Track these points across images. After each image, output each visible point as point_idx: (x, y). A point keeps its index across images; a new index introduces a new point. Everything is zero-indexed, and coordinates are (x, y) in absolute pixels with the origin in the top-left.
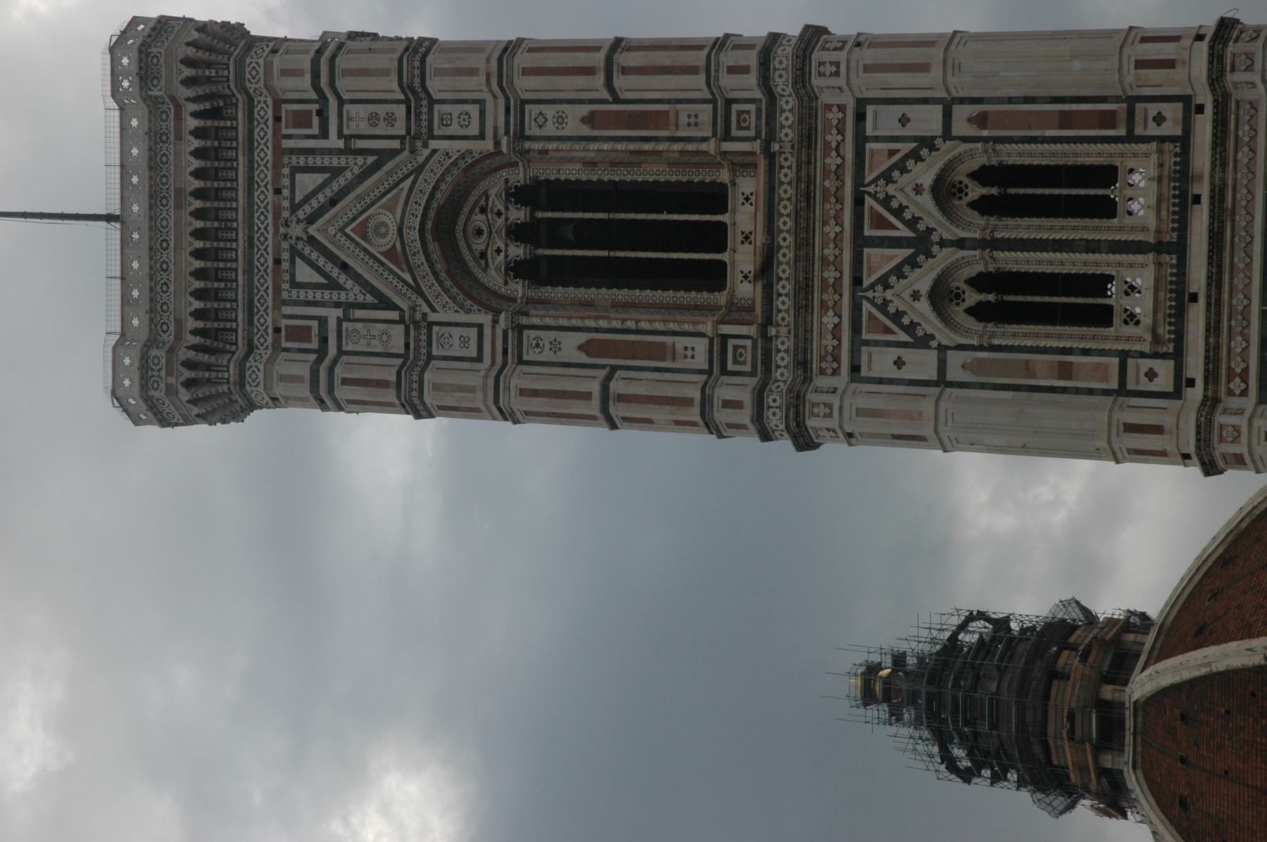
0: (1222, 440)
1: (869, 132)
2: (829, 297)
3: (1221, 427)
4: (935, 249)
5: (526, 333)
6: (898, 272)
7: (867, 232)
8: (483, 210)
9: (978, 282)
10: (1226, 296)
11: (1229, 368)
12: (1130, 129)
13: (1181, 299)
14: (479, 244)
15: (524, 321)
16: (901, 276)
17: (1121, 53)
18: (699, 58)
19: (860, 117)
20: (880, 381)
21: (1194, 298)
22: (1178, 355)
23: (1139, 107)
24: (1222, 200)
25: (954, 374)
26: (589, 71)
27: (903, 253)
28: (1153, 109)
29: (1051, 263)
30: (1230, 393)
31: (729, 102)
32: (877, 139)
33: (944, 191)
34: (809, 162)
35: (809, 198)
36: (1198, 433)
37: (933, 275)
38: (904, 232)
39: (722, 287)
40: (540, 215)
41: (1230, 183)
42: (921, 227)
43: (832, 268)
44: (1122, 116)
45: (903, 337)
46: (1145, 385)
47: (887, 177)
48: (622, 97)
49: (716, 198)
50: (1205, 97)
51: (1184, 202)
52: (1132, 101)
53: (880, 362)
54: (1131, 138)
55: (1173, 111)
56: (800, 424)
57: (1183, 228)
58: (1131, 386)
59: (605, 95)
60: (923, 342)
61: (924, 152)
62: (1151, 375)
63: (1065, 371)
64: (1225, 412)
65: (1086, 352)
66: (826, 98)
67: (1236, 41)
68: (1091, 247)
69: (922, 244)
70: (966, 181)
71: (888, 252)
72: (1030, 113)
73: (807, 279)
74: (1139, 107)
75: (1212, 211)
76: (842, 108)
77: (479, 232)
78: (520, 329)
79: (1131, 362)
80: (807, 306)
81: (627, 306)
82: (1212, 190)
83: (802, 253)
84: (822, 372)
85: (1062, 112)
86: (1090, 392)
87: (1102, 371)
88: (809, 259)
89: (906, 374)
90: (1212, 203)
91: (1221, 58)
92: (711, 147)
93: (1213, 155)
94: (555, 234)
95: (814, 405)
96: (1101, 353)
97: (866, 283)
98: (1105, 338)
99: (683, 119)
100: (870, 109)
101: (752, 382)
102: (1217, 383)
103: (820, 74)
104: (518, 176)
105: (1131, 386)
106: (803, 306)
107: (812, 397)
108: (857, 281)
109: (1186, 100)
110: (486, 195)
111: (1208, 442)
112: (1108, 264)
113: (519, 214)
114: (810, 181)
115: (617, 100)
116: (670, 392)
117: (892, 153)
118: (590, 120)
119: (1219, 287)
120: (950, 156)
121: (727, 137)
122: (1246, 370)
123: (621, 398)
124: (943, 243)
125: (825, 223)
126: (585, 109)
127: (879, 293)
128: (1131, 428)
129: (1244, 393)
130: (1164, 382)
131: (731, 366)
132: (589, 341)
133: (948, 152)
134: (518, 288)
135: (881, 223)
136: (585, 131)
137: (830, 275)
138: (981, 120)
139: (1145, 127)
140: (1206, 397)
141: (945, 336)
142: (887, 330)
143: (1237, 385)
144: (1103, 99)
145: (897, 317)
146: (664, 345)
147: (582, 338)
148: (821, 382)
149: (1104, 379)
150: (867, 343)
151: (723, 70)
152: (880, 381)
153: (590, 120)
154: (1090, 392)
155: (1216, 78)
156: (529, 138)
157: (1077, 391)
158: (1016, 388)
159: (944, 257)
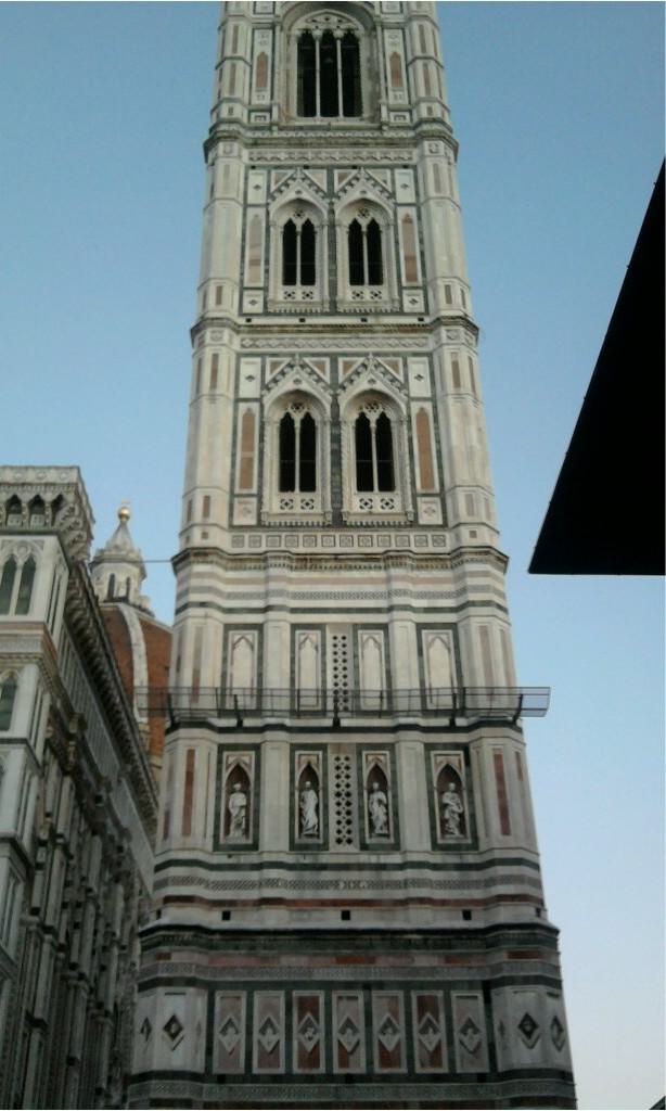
0: (213, 332)
1: (397, 171)
2: (296, 156)
3: (221, 332)
4: (328, 200)
5: (271, 32)
6: (312, 184)
7: (336, 172)
8: (340, 21)
9: (308, 226)
10: (304, 335)
11: (258, 339)
12: (405, 288)
13: (302, 316)
14: (321, 19)
15: (278, 28)
16: (310, 186)
17: (455, 277)
18: (435, 93)
19: (405, 167)
20: (246, 179)
21: (302, 320)
22: (266, 313)
23: (421, 292)
24: (364, 332)
25: (251, 212)
26: (424, 48)
27: (325, 188)
28: (420, 299)
29: (322, 255)
30: (243, 340)
31: (410, 112)
32: (393, 175)
33: (365, 204)
34: (377, 144)
35: (355, 144)
36: (217, 319)
37: (312, 200)
38: (337, 187)
39: (299, 114)
40: (339, 43)
41: (375, 335)
42: (341, 194)
43: (314, 156)
44: (415, 284)
45: (273, 188)
46: (246, 300)
47: (370, 178)
48: (410, 69)
49: (353, 109)
50: (427, 320)
51: (364, 315)
52: (425, 289)
53: (257, 178)
54: (401, 288)
55: (420, 307)
56: (219, 139)
57: (345, 314)
58: (246, 293)
59: (410, 58)
60: (271, 196)
61: (387, 194)
62: (253, 302)
63: (255, 262)
64: (231, 336)
65: (267, 271)
66: (416, 152)
67: (466, 334)
68: (333, 272)
69: (331, 194)
70: (369, 218)
71: (325, 181)
72: (414, 242)
73: (307, 144)
74: (421, 292)
75: (358, 326)
76: (410, 159)
77: (327, 19)
78: (273, 27)
79: (261, 292)
80: (290, 144)
81: (288, 76)
82: (371, 326)
83: (322, 141)
84: (251, 153)
85: (414, 258)
86: (242, 274)
87: (257, 278)
88: (319, 146)
89: (251, 191)
90: (362, 326)
91: (456, 324)
92: (383, 100)
93: (393, 325)
94: (328, 52)
95: (231, 146)
96: (267, 279)
97: (306, 172)
98: (276, 282)
99: (398, 93)
100: (410, 171)
101: (245, 120)
102: (249, 332)
103: (430, 145)
104: (360, 32)
105: (246, 293)
106: (289, 143)
107: (236, 145)
108: (306, 167)
109: (427, 312)
110: (349, 21)
111: (212, 325)
112: (322, 281)
113: (339, 33)
114: (366, 145)
115: (407, 66)
116: (239, 85)
117: (385, 182)
118: (395, 56)
119: (310, 332)
120: (385, 206)
121: (390, 110)
122: (257, 347)
123: (234, 66)
124: (331, 204)
125: (341, 153)
126: (401, 52)
127: (299, 175)
128: (219, 290)
129: (243, 346)
130: (248, 308)
131: (253, 115)
132: (266, 57)
133: (388, 205)
134: (296, 32)
135: (341, 178)
136: (389, 52)
137: (310, 156)
138: (408, 220)
139: (409, 295)
140: (240, 326)
141: (273, 207)
142: (276, 182)
143: (248, 342)
144: (424, 274)
145: (287, 185)
146: (266, 86)
147: (269, 52)
148: (245, 153)
149: (250, 280)
150: (269, 172)
151: (429, 104)
152: (246, 179)
153: (395, 56)
154: (242, 274)
155: (439, 321)
156: (383, 29)
157: (242, 267)
158: (244, 239)
159: (323, 205)
